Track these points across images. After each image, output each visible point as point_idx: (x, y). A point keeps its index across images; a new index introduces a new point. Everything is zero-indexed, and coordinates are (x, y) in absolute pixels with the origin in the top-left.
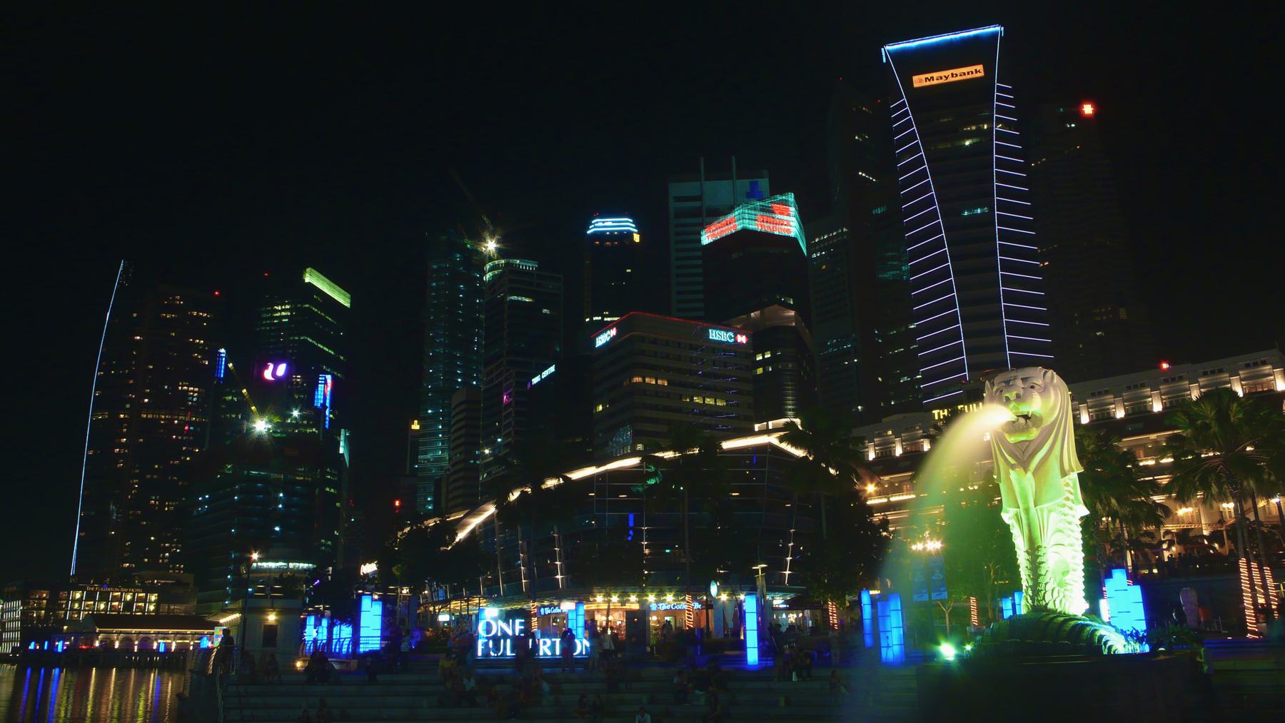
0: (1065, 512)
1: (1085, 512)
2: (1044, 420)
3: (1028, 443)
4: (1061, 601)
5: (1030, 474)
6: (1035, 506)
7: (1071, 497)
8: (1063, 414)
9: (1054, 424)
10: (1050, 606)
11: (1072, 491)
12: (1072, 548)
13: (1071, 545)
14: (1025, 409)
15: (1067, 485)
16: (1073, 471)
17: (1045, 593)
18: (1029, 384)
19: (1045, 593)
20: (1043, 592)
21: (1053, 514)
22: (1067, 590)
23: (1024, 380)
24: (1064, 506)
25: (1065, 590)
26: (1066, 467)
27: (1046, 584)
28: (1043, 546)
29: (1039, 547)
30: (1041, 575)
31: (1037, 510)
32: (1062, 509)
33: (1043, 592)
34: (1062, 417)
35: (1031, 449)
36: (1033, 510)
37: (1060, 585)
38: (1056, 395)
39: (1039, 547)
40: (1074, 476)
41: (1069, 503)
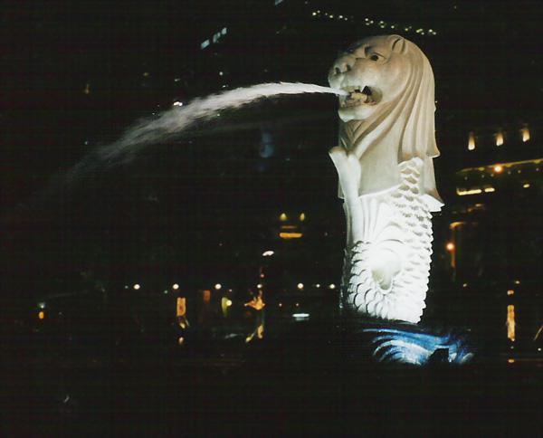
0: (402, 203)
1: (437, 206)
2: (384, 98)
3: (360, 123)
4: (376, 305)
5: (351, 158)
6: (360, 195)
8: (412, 87)
9: (395, 103)
10: (363, 308)
11: (417, 179)
13: (408, 241)
15: (409, 172)
20: (352, 296)
21: (383, 205)
22: (394, 293)
23: (367, 50)
24: (399, 196)
26: (407, 147)
32: (396, 200)
37: (384, 287)
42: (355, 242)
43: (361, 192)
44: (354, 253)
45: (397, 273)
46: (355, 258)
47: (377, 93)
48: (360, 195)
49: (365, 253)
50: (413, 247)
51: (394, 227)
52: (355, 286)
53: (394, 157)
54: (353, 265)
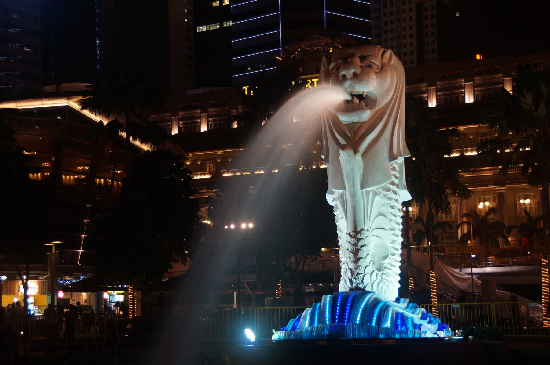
2: (378, 103)
4: (378, 284)
5: (359, 157)
6: (361, 189)
7: (397, 181)
11: (398, 175)
12: (393, 232)
14: (362, 88)
15: (394, 169)
16: (401, 155)
17: (364, 277)
18: (366, 63)
19: (364, 277)
20: (362, 275)
21: (377, 198)
23: (363, 58)
24: (389, 190)
25: (383, 274)
27: (366, 267)
28: (366, 229)
29: (362, 230)
30: (361, 258)
31: (362, 193)
32: (386, 193)
33: (362, 275)
34: (396, 99)
35: (362, 132)
36: (359, 192)
37: (379, 269)
38: (392, 76)
39: (362, 230)
40: (401, 160)
41: (394, 188)
42: (359, 229)
43: (362, 188)
44: (359, 240)
45: (386, 257)
46: (360, 243)
47: (371, 98)
48: (361, 189)
49: (367, 239)
50: (395, 235)
51: (382, 217)
52: (363, 268)
53: (385, 154)
54: (360, 249)
